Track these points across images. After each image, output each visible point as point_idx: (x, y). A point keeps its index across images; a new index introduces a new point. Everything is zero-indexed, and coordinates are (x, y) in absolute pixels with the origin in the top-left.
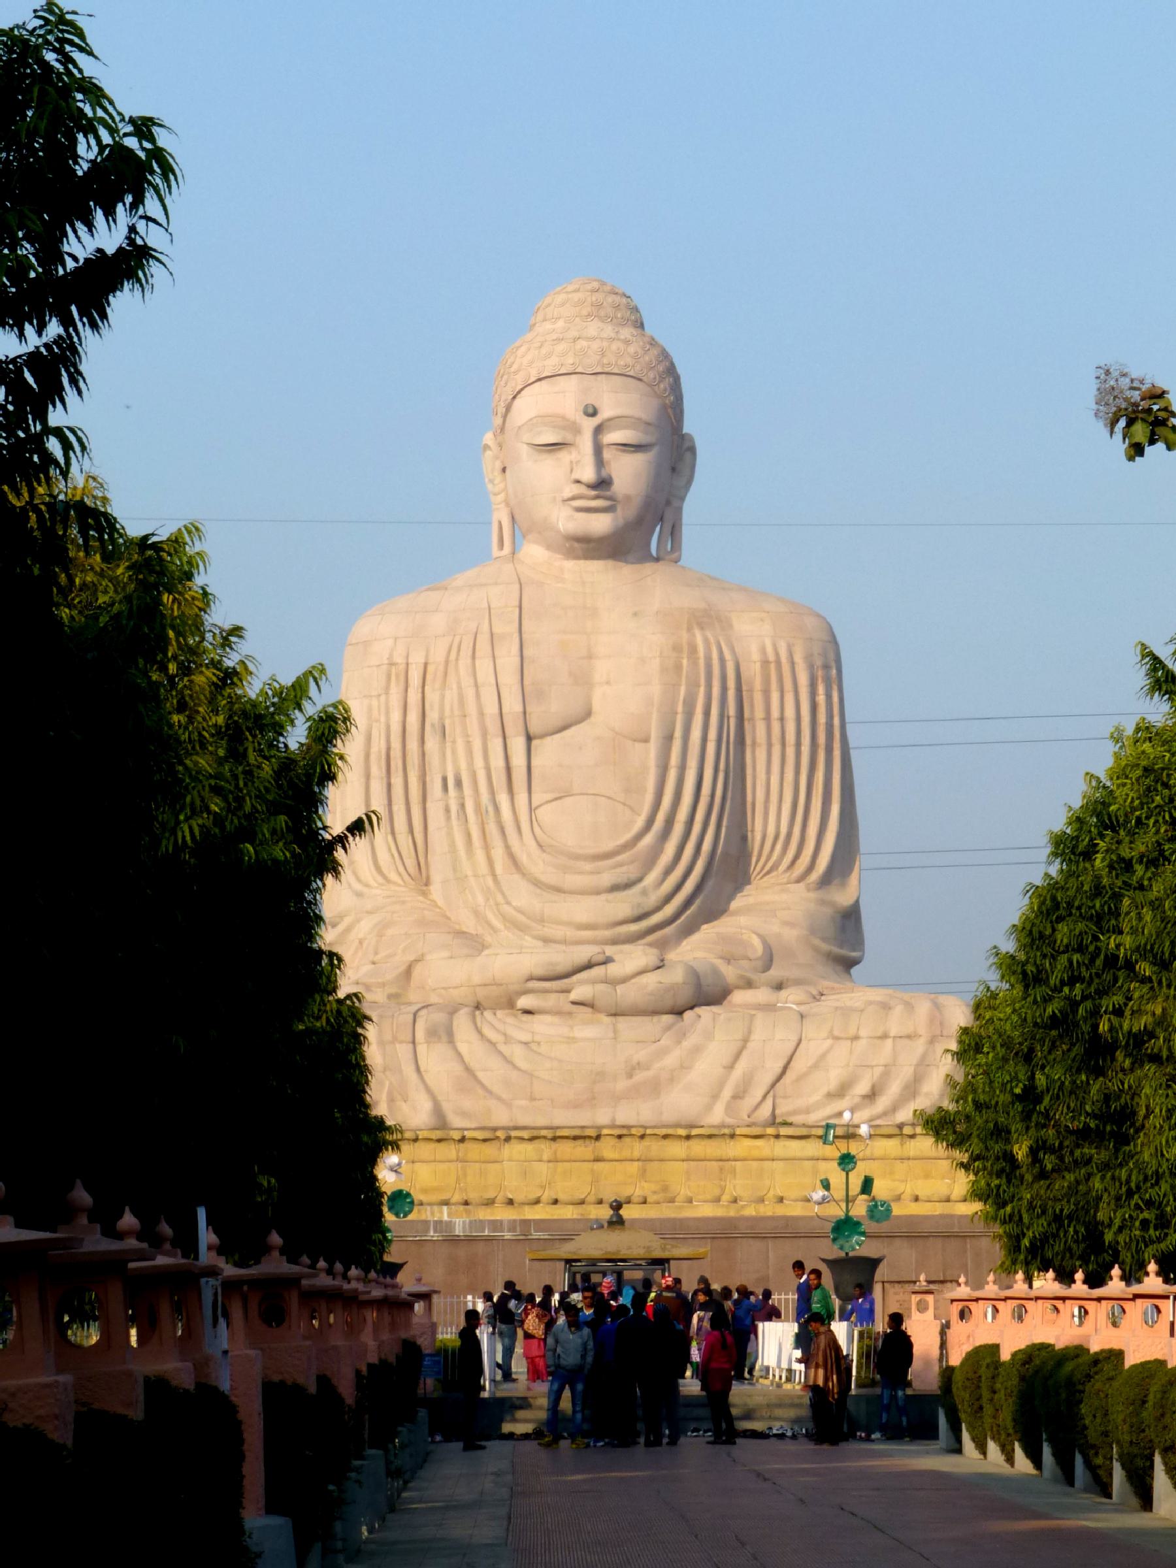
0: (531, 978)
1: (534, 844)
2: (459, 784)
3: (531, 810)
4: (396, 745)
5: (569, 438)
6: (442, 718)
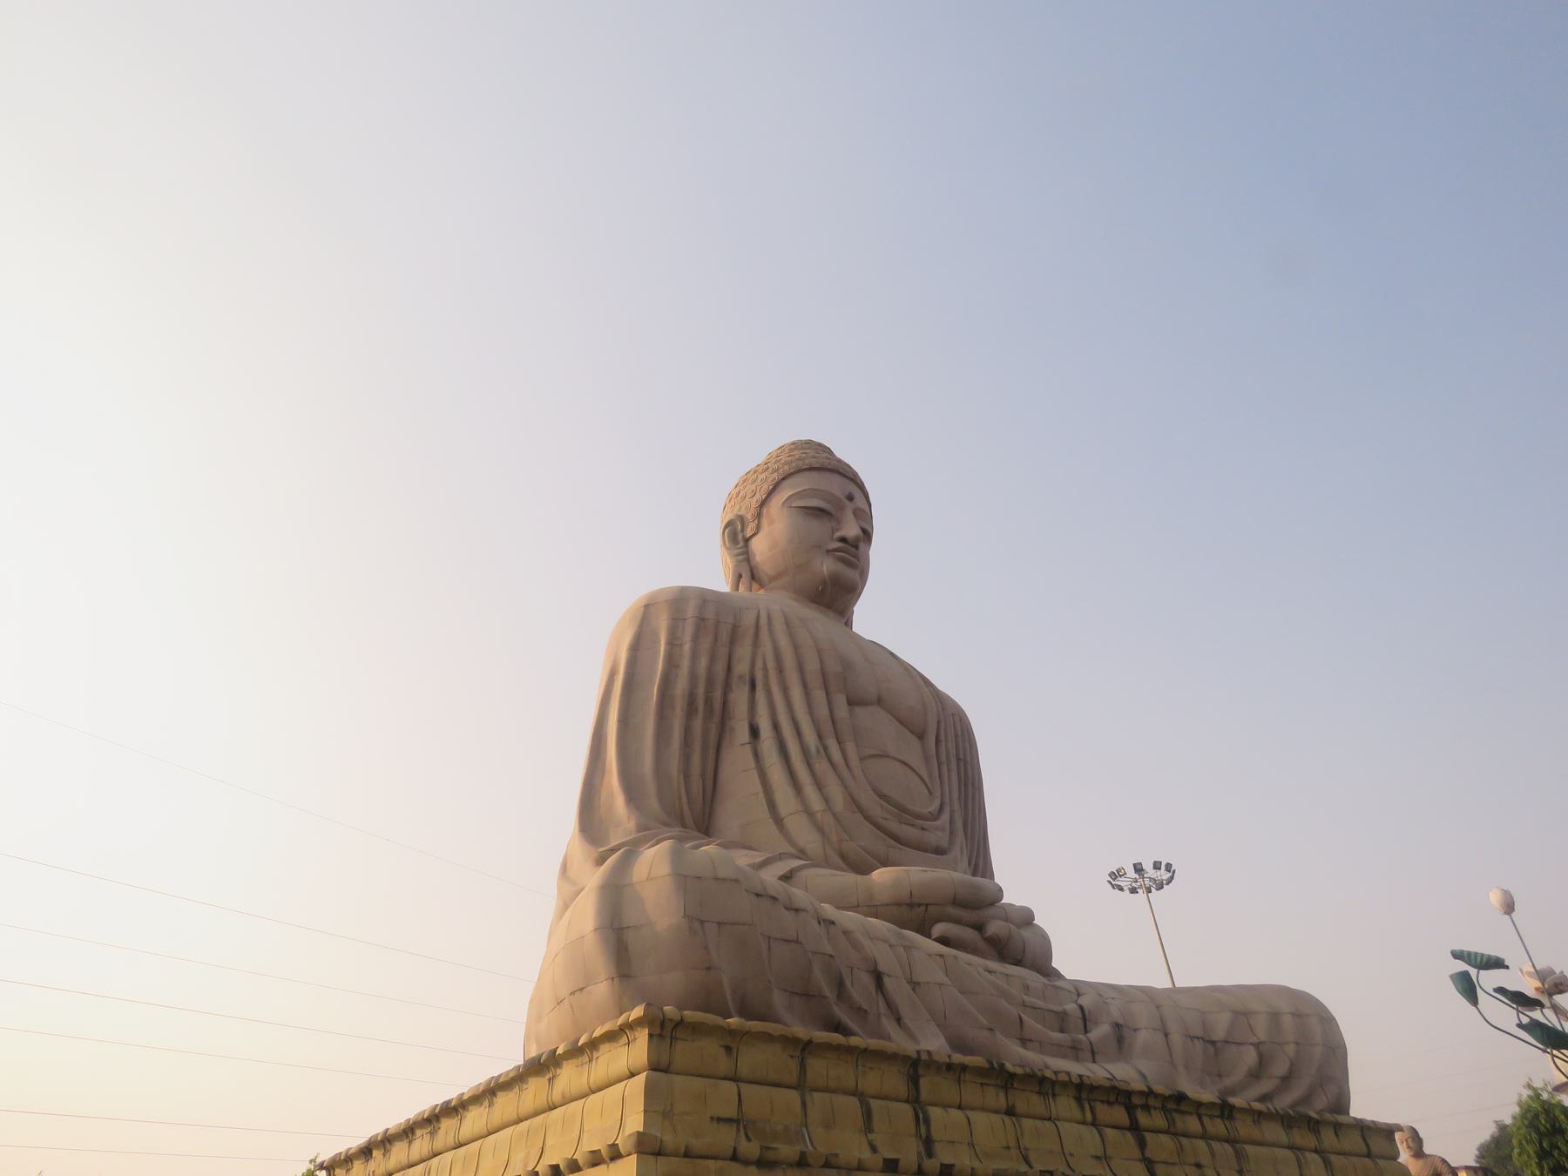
0: (957, 902)
4: (701, 690)
5: (832, 510)
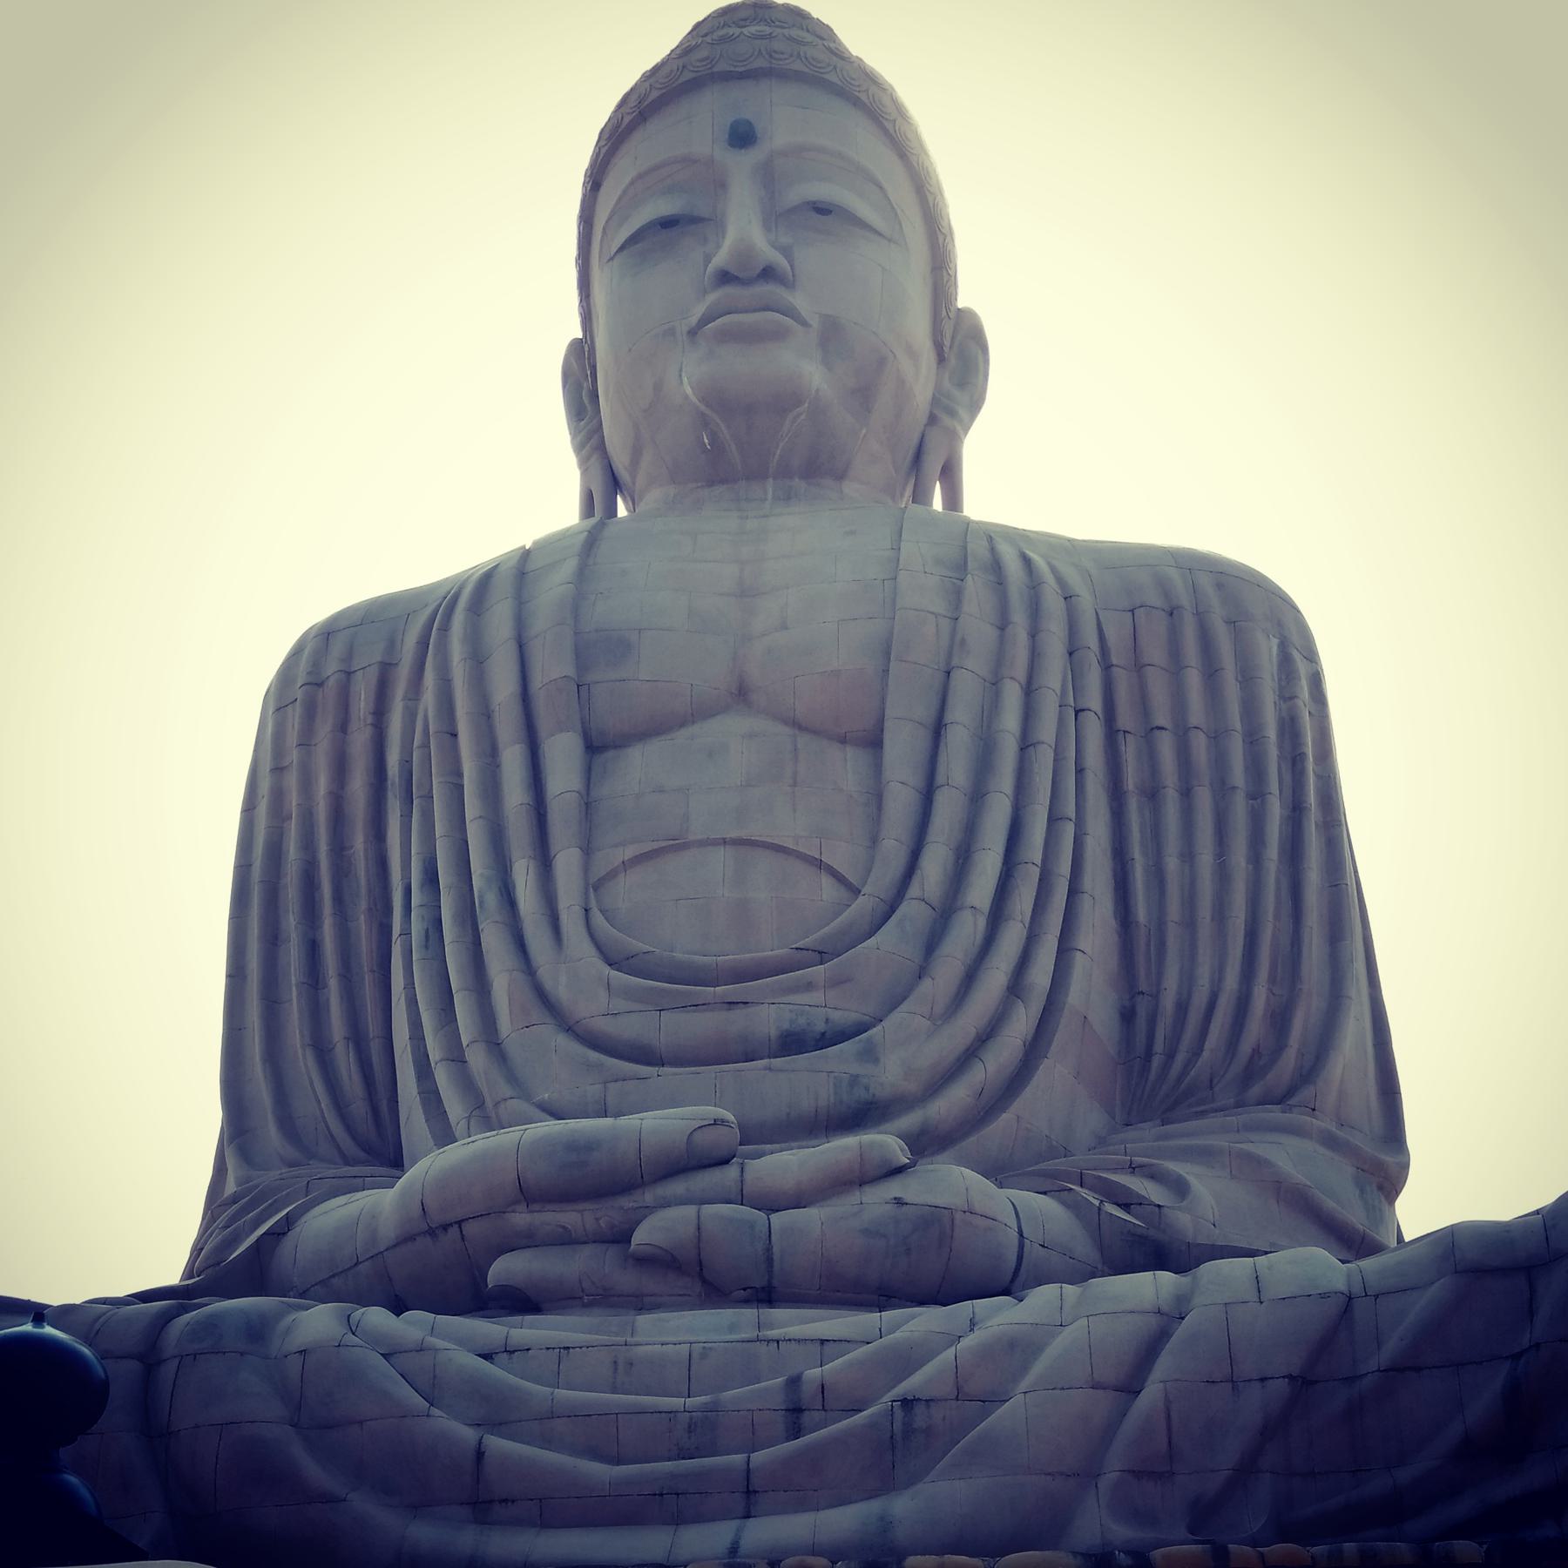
0: (529, 1194)
1: (587, 949)
2: (431, 878)
3: (594, 886)
6: (406, 764)
